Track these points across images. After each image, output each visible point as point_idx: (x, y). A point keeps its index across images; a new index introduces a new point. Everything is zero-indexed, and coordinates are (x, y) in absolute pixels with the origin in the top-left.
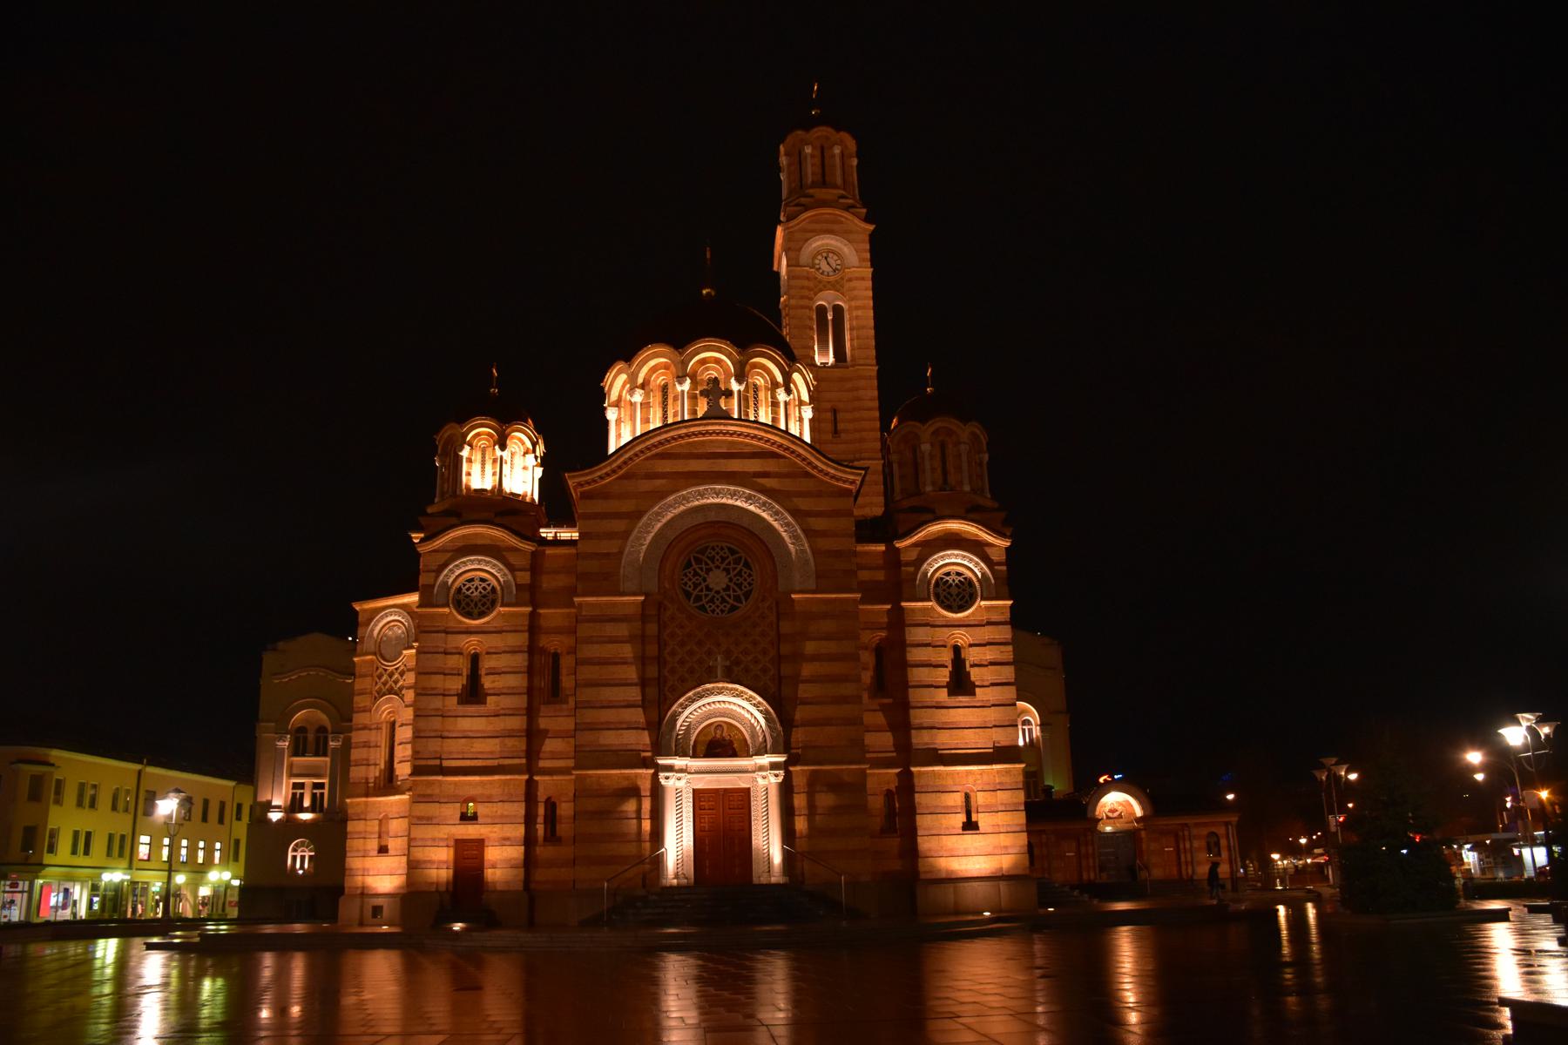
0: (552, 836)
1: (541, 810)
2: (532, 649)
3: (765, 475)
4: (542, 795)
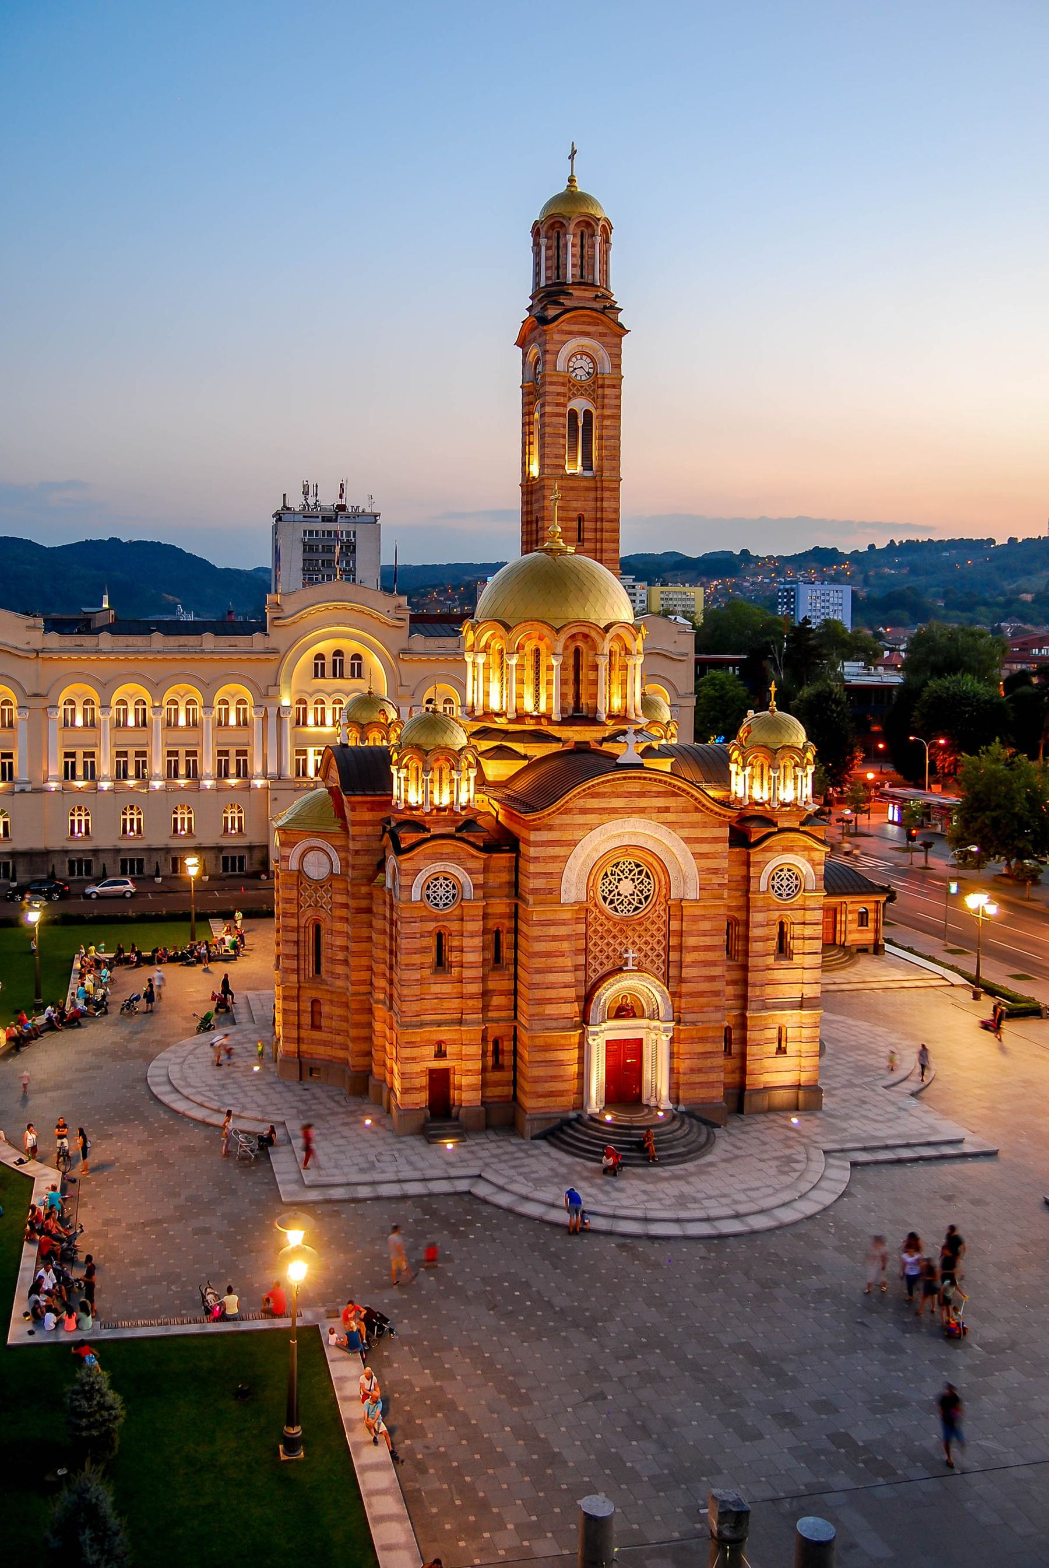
0: (498, 1066)
1: (490, 1047)
2: (485, 931)
3: (667, 810)
4: (491, 1039)
